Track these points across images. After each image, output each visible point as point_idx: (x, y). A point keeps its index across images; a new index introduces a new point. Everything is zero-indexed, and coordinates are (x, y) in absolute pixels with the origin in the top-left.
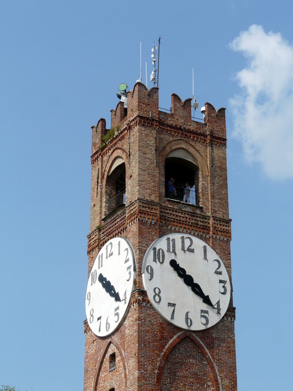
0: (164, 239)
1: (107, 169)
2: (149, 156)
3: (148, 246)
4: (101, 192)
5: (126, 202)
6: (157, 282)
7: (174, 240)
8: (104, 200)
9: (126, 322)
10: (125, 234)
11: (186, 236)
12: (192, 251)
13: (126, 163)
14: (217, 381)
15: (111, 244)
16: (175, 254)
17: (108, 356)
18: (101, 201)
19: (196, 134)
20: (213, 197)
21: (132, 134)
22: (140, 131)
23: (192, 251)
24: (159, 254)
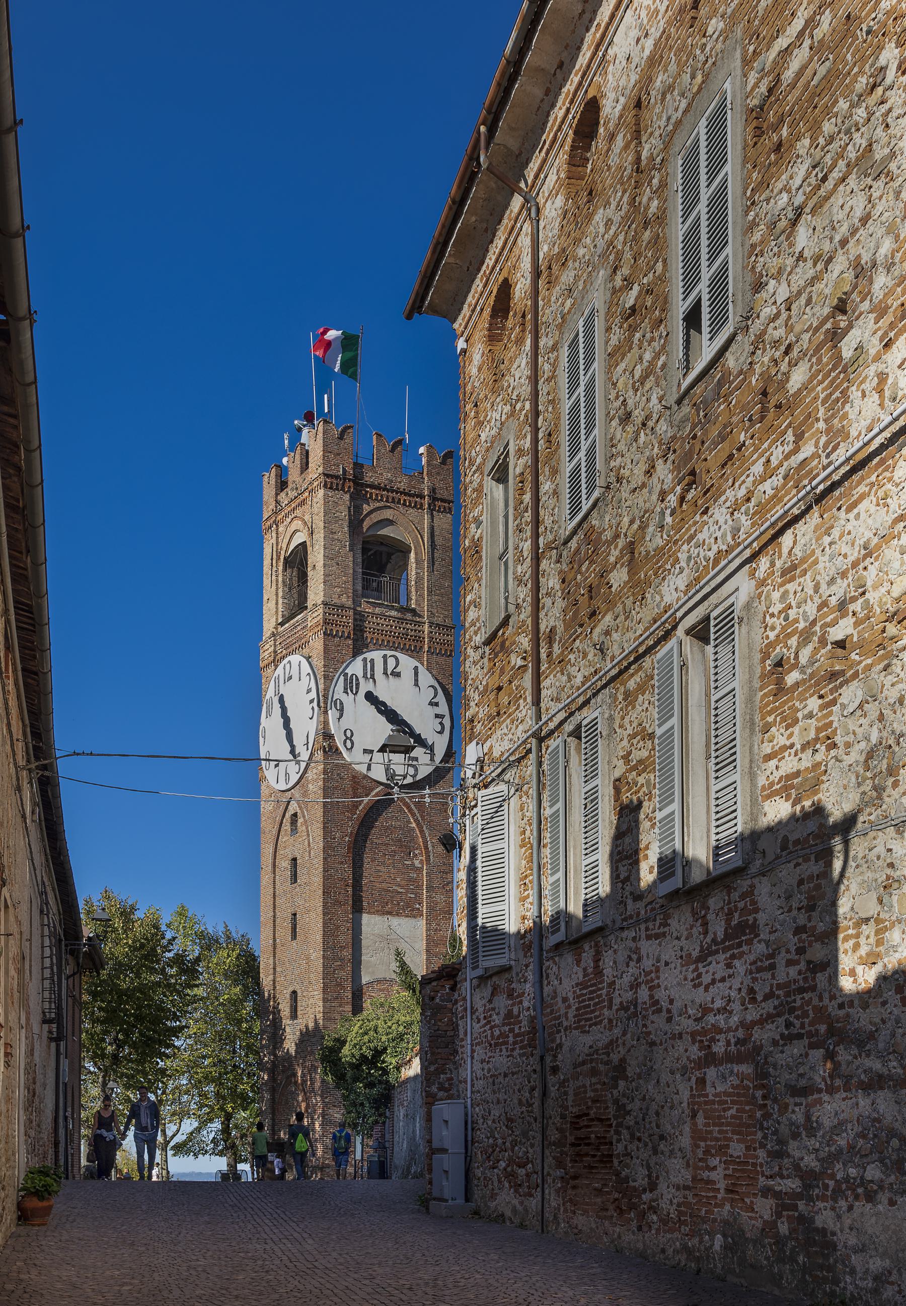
0: (359, 661)
1: (284, 546)
2: (339, 535)
3: (336, 670)
4: (277, 581)
5: (310, 604)
6: (346, 722)
7: (372, 661)
8: (280, 594)
9: (310, 775)
10: (305, 651)
11: (389, 653)
12: (398, 675)
13: (308, 543)
14: (426, 848)
15: (289, 662)
16: (375, 681)
17: (288, 815)
18: (277, 595)
19: (410, 495)
20: (430, 592)
21: (315, 500)
22: (326, 496)
23: (398, 675)
24: (351, 683)
